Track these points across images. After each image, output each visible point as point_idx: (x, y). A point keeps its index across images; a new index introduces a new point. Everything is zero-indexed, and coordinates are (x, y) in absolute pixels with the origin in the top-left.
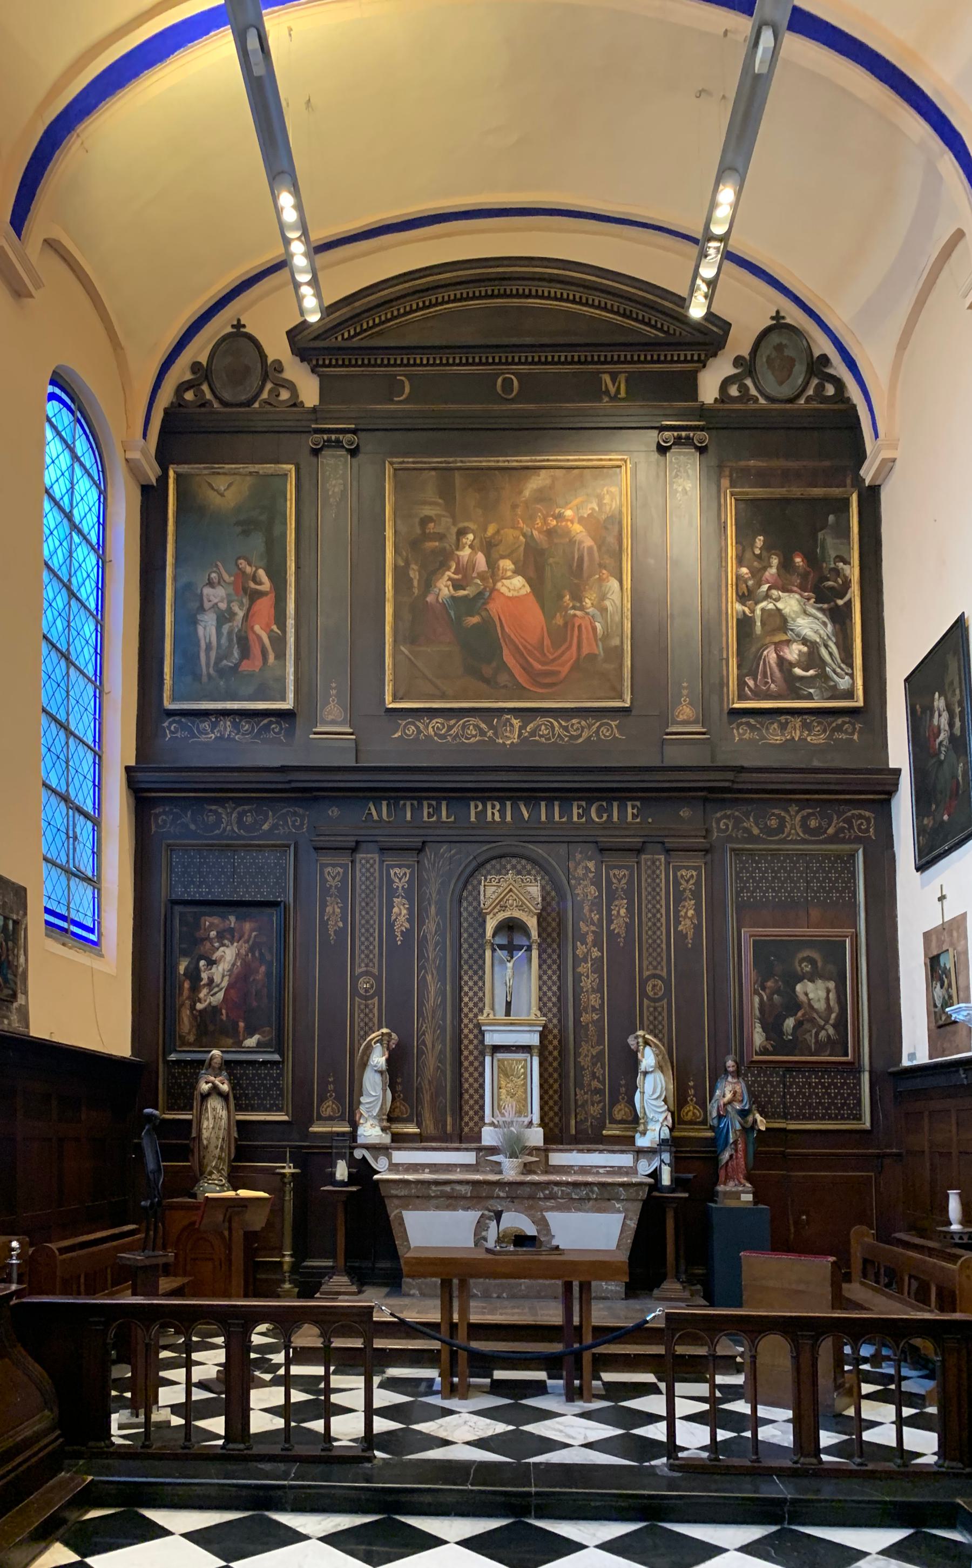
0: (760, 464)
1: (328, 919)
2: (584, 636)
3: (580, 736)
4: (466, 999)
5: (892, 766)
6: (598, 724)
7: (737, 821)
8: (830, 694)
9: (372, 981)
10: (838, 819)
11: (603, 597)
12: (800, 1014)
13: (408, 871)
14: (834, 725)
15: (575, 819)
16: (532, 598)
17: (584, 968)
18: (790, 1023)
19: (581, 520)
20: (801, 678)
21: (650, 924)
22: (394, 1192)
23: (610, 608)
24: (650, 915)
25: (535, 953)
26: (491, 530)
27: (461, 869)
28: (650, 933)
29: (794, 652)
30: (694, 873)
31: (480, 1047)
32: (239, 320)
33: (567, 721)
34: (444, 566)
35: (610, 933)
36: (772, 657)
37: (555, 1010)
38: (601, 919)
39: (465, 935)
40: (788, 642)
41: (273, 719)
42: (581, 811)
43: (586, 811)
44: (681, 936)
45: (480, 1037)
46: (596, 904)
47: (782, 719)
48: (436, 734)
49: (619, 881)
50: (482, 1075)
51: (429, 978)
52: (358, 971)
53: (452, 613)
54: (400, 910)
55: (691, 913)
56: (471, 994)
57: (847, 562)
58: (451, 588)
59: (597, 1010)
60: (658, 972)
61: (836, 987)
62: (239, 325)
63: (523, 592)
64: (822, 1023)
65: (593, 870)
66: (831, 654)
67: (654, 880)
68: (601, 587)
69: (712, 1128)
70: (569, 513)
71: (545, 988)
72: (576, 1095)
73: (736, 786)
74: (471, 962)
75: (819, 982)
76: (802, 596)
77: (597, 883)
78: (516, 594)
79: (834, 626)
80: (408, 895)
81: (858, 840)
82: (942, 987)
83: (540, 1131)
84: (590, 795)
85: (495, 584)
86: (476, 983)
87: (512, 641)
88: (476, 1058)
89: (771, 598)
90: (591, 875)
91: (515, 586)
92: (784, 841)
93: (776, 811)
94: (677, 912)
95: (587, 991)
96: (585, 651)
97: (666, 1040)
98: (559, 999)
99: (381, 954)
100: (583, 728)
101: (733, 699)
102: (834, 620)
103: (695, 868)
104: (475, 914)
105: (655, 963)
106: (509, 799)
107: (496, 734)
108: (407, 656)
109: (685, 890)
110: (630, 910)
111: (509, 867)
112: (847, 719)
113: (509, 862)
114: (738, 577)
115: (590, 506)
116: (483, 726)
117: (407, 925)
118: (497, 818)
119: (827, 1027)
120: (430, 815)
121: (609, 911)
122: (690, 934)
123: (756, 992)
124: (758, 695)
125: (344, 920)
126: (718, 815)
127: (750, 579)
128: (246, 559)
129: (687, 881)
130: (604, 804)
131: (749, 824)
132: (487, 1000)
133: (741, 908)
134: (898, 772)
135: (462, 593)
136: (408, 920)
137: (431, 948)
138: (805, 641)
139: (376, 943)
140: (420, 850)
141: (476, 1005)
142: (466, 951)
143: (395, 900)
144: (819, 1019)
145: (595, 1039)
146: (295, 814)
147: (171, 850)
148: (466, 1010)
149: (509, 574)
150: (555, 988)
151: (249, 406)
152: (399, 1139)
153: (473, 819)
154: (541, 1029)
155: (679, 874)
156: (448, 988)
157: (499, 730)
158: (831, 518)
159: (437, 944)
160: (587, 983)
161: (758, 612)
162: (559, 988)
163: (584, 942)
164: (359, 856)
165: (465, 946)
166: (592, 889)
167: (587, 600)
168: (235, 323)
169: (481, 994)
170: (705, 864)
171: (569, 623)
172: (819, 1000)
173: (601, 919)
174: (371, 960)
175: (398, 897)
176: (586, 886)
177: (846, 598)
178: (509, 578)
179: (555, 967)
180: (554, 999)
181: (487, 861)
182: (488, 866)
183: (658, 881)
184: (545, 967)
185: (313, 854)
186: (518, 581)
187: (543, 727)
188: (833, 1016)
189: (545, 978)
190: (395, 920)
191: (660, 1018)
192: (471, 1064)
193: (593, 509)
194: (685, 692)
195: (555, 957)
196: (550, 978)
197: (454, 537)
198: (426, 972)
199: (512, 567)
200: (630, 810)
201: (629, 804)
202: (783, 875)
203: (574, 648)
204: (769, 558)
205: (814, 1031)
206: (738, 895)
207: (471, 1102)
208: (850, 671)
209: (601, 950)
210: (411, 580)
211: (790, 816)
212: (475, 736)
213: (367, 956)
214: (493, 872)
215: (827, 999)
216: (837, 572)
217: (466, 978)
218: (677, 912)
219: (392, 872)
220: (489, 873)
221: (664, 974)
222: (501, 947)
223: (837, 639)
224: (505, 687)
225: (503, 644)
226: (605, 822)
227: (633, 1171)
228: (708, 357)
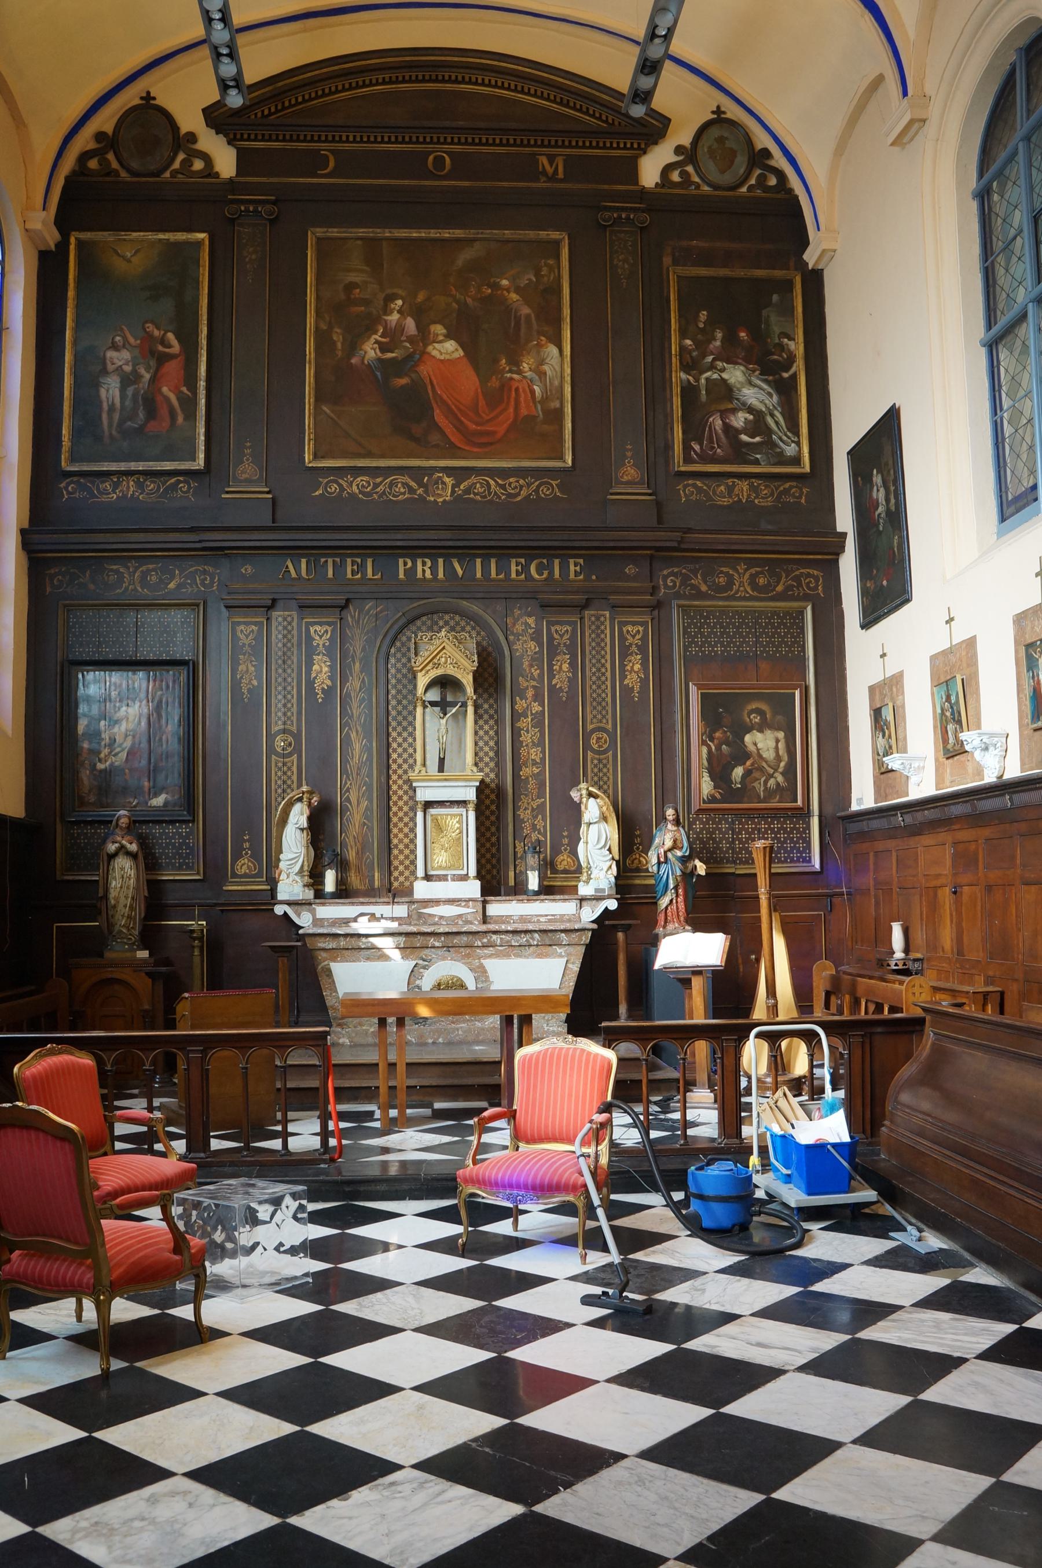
0: (701, 244)
1: (241, 678)
2: (522, 399)
3: (519, 494)
4: (394, 756)
5: (839, 529)
6: (537, 483)
7: (685, 579)
8: (776, 460)
9: (290, 739)
10: (786, 577)
11: (542, 362)
13: (329, 629)
14: (782, 488)
15: (513, 575)
16: (465, 360)
19: (518, 290)
20: (748, 444)
22: (321, 945)
23: (549, 373)
24: (594, 670)
25: (470, 710)
26: (421, 297)
27: (388, 625)
28: (594, 687)
29: (739, 420)
30: (641, 629)
32: (148, 93)
33: (504, 479)
34: (371, 330)
35: (552, 689)
36: (719, 423)
37: (492, 765)
40: (734, 411)
41: (181, 479)
42: (519, 568)
43: (526, 569)
44: (627, 691)
45: (410, 793)
46: (537, 659)
47: (730, 481)
48: (360, 492)
49: (562, 636)
51: (353, 735)
52: (275, 729)
53: (378, 374)
54: (322, 670)
55: (637, 667)
56: (400, 750)
57: (791, 339)
58: (378, 350)
62: (148, 97)
63: (456, 355)
65: (533, 626)
66: (777, 423)
67: (598, 636)
68: (538, 352)
70: (505, 282)
71: (481, 744)
73: (683, 546)
74: (400, 718)
76: (747, 368)
77: (537, 637)
78: (448, 357)
79: (780, 398)
80: (330, 652)
81: (806, 598)
82: (884, 736)
83: (478, 883)
84: (530, 552)
85: (425, 346)
87: (444, 402)
89: (716, 368)
91: (448, 349)
92: (733, 598)
93: (724, 569)
94: (622, 666)
95: (527, 745)
96: (524, 412)
97: (611, 792)
98: (497, 753)
99: (299, 713)
100: (521, 487)
101: (679, 462)
102: (779, 392)
103: (641, 624)
104: (404, 671)
106: (441, 556)
107: (426, 492)
108: (329, 416)
109: (631, 645)
110: (573, 665)
111: (441, 623)
112: (794, 484)
113: (442, 618)
114: (682, 349)
115: (527, 276)
116: (413, 484)
117: (329, 683)
118: (428, 575)
120: (353, 573)
122: (637, 688)
124: (704, 459)
125: (259, 678)
126: (665, 572)
127: (694, 350)
128: (152, 322)
129: (633, 637)
130: (545, 561)
131: (697, 581)
132: (419, 757)
133: (687, 661)
134: (844, 535)
135: (390, 355)
136: (330, 678)
137: (355, 704)
138: (750, 410)
139: (295, 701)
140: (344, 607)
141: (405, 761)
146: (205, 572)
147: (68, 610)
148: (394, 766)
149: (441, 338)
150: (492, 743)
151: (158, 176)
153: (401, 576)
155: (625, 629)
157: (430, 488)
158: (775, 298)
160: (526, 738)
161: (703, 381)
162: (497, 743)
163: (523, 697)
164: (275, 614)
165: (393, 702)
167: (525, 365)
168: (144, 95)
169: (411, 750)
170: (652, 619)
171: (506, 385)
174: (289, 718)
175: (318, 654)
176: (525, 641)
177: (791, 372)
178: (440, 342)
179: (492, 722)
180: (491, 754)
181: (418, 617)
182: (419, 623)
183: (603, 636)
184: (481, 722)
185: (225, 612)
186: (450, 346)
187: (478, 485)
189: (481, 733)
190: (315, 678)
191: (605, 770)
193: (530, 280)
194: (629, 454)
195: (492, 712)
196: (486, 733)
197: (382, 303)
198: (350, 729)
199: (444, 331)
200: (572, 568)
201: (572, 561)
202: (731, 631)
203: (511, 410)
204: (714, 331)
206: (685, 651)
208: (796, 439)
209: (542, 705)
210: (334, 343)
211: (739, 574)
212: (404, 494)
213: (285, 714)
214: (424, 628)
216: (781, 347)
217: (394, 734)
218: (622, 666)
219: (312, 630)
220: (419, 629)
223: (782, 408)
224: (437, 446)
225: (435, 406)
226: (546, 579)
228: (647, 145)
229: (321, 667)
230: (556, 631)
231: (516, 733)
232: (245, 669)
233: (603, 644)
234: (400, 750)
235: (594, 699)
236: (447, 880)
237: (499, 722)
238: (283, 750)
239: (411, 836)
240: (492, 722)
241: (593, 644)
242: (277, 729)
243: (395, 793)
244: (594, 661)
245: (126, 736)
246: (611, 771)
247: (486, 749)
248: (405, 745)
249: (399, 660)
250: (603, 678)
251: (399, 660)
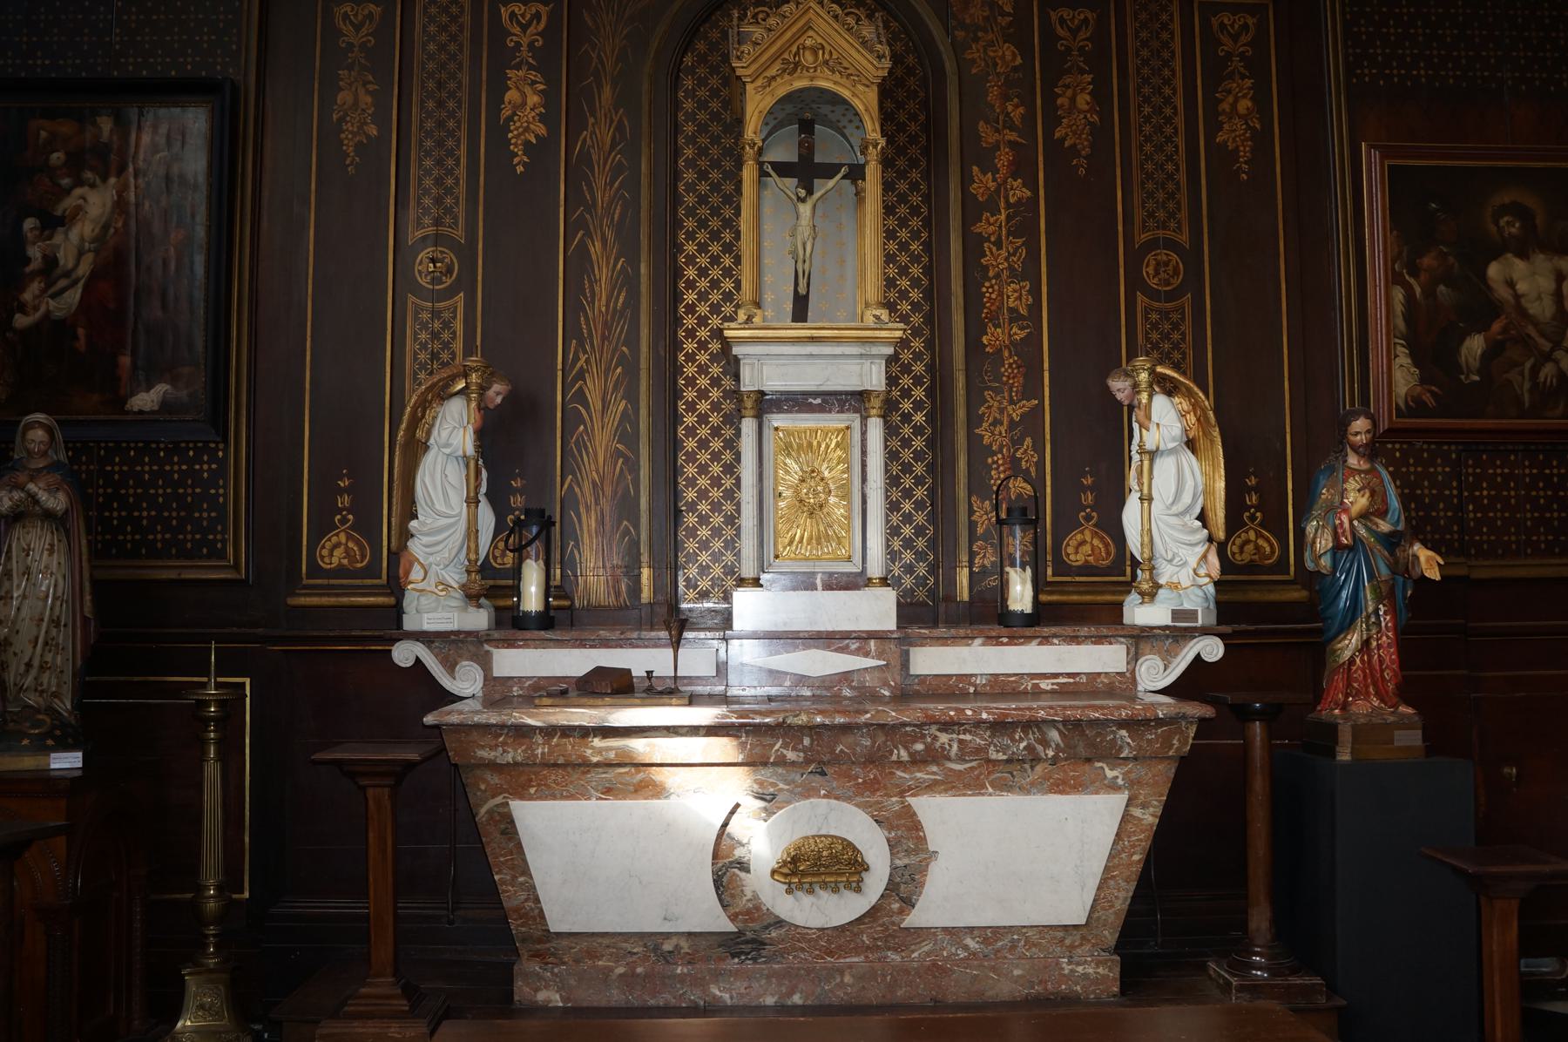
1: (342, 120)
9: (450, 257)
12: (1496, 326)
17: (992, 224)
18: (1475, 345)
21: (1147, 129)
24: (1147, 110)
28: (1148, 148)
31: (728, 406)
38: (1030, 118)
39: (689, 152)
50: (731, 469)
51: (595, 249)
52: (414, 235)
54: (525, 100)
55: (1244, 105)
56: (703, 284)
59: (1022, 318)
60: (1169, 234)
64: (1546, 346)
65: (1008, 9)
69: (1310, 579)
72: (971, 512)
74: (703, 211)
80: (544, 62)
86: (715, 260)
88: (716, 432)
90: (1004, 21)
95: (997, 276)
105: (1161, 214)
110: (1101, 96)
117: (541, 129)
121: (1050, 98)
122: (1245, 153)
125: (381, 119)
136: (543, 118)
137: (600, 181)
139: (462, 172)
142: (691, 188)
143: (511, 73)
144: (1541, 341)
145: (1017, 383)
150: (916, 271)
152: (513, 625)
154: (890, 351)
156: (643, 269)
159: (617, 170)
162: (928, 271)
163: (988, 167)
166: (1008, 50)
173: (1030, 118)
174: (448, 211)
175: (518, 67)
179: (915, 223)
180: (915, 295)
190: (510, 119)
191: (1176, 336)
192: (703, 444)
198: (588, 234)
205: (1528, 365)
207: (704, 532)
221: (1184, 238)
222: (783, 169)
227: (1123, 687)
229: (524, 96)
230: (1062, 21)
231: (973, 248)
232: (350, 100)
233: (1166, 55)
234: (703, 284)
235: (1149, 176)
236: (813, 587)
237: (935, 224)
238: (434, 281)
239: (728, 483)
240: (915, 223)
241: (1145, 53)
242: (419, 234)
243: (691, 382)
244: (1146, 90)
245: (81, 254)
246: (1189, 338)
247: (904, 283)
248: (715, 273)
249: (702, 82)
250: (1168, 130)
251: (702, 82)
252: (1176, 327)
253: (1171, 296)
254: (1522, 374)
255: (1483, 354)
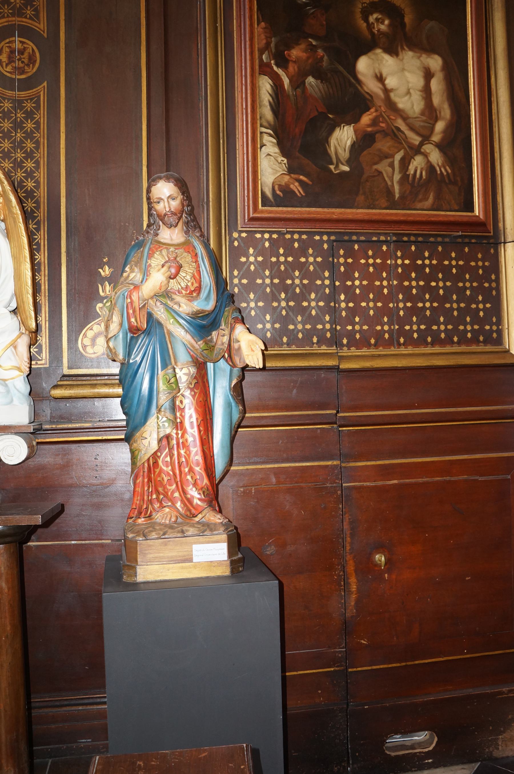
12: (366, 119)
18: (343, 138)
61: (446, 67)
64: (416, 140)
75: (409, 57)
119: (428, 148)
123: (265, 69)
172: (408, 93)
188: (440, 126)
205: (398, 157)
215: (427, 91)
252: (29, 115)
253: (27, 84)
254: (392, 165)
255: (353, 145)
